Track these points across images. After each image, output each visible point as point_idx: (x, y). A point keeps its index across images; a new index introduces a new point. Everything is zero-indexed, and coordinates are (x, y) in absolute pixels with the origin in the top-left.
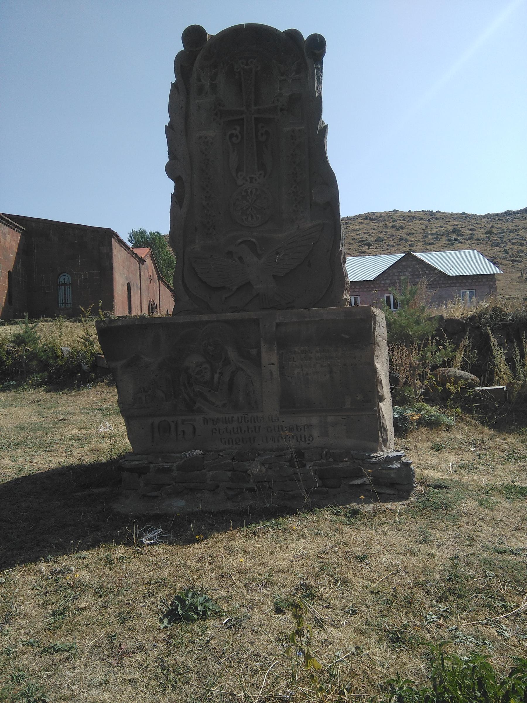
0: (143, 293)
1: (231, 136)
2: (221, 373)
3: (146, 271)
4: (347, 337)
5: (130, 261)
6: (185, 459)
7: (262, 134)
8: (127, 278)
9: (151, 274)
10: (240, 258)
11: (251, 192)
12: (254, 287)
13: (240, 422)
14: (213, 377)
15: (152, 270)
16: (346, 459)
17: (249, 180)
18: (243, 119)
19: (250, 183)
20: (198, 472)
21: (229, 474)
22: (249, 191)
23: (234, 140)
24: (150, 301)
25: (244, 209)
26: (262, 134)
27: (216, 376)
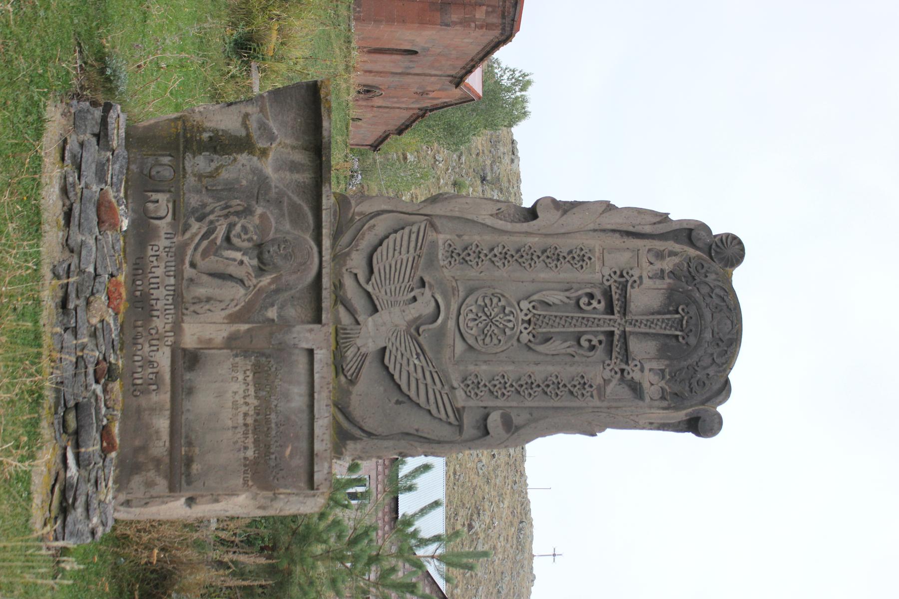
0: (396, 79)
1: (591, 296)
2: (241, 263)
3: (438, 87)
4: (288, 452)
5: (457, 58)
6: (116, 204)
7: (590, 341)
8: (426, 50)
9: (431, 95)
10: (415, 299)
11: (510, 321)
12: (370, 319)
13: (167, 288)
14: (238, 249)
15: (440, 98)
16: (105, 444)
17: (527, 318)
18: (612, 313)
19: (522, 320)
20: (96, 223)
21: (91, 269)
22: (511, 318)
23: (584, 300)
24: (380, 89)
25: (486, 309)
26: (590, 341)
27: (238, 255)
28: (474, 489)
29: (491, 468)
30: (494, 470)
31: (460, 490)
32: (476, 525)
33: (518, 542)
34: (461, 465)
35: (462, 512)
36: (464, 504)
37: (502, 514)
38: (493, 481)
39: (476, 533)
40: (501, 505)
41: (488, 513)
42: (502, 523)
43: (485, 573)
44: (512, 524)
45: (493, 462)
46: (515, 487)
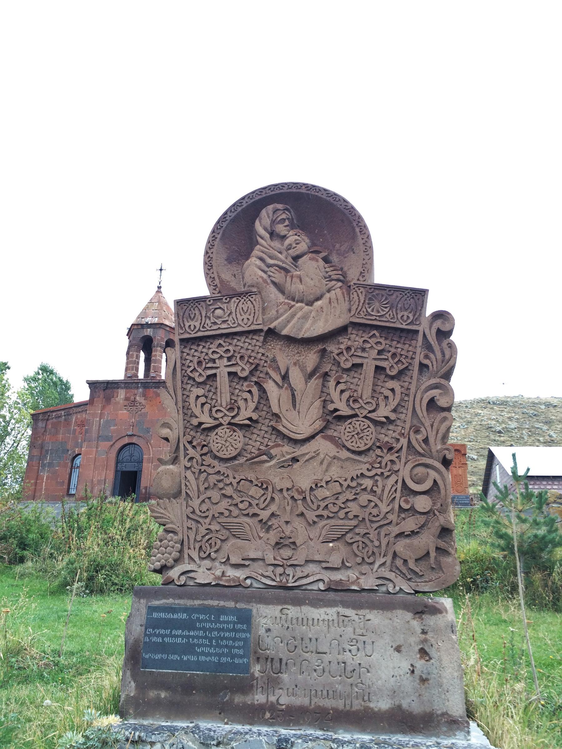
28: (477, 430)
29: (461, 421)
30: (462, 418)
31: (479, 438)
32: (499, 429)
33: (501, 405)
34: (464, 438)
35: (492, 437)
36: (487, 436)
37: (487, 414)
38: (469, 419)
39: (503, 429)
40: (482, 414)
41: (489, 422)
42: (493, 414)
43: (526, 423)
44: (492, 408)
45: (458, 419)
46: (469, 407)
